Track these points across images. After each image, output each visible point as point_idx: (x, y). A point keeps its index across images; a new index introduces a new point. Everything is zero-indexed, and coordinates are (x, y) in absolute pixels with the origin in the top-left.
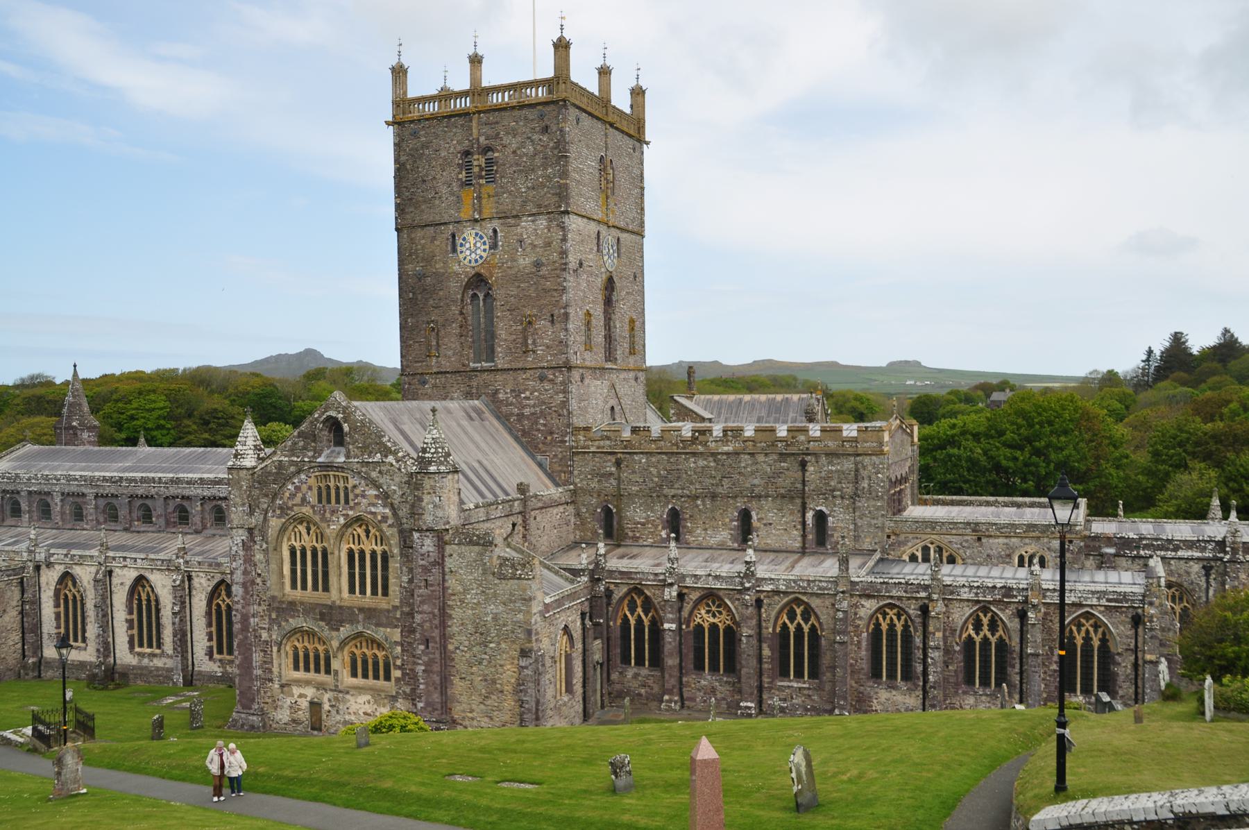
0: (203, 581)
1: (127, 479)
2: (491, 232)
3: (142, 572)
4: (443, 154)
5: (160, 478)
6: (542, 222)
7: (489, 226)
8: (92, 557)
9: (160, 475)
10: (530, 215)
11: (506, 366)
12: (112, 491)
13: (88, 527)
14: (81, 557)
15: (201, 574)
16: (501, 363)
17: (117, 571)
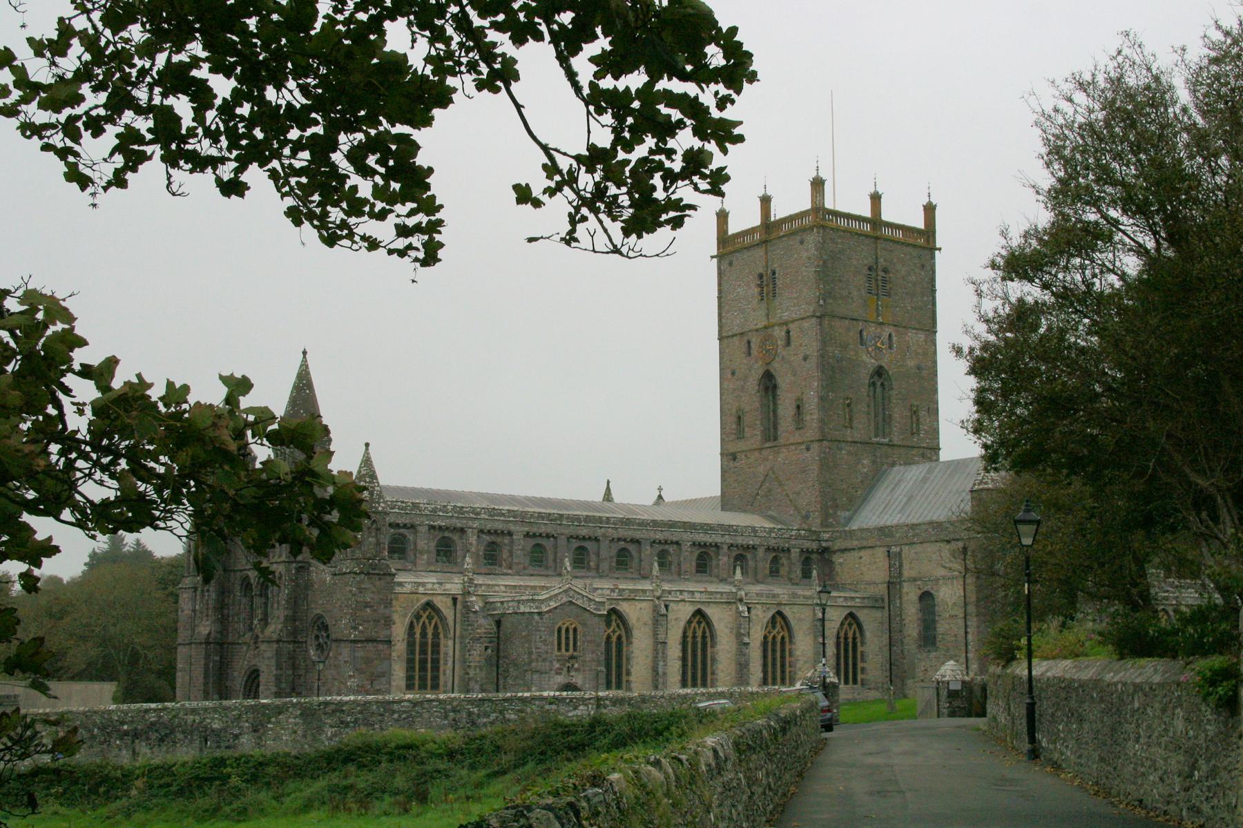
0: (760, 612)
1: (568, 517)
2: (885, 336)
3: (699, 606)
4: (855, 262)
5: (608, 518)
6: (922, 336)
7: (888, 330)
8: (644, 591)
9: (608, 515)
10: (915, 329)
11: (900, 443)
12: (550, 530)
13: (510, 571)
14: (631, 591)
15: (758, 606)
16: (896, 441)
17: (672, 605)
